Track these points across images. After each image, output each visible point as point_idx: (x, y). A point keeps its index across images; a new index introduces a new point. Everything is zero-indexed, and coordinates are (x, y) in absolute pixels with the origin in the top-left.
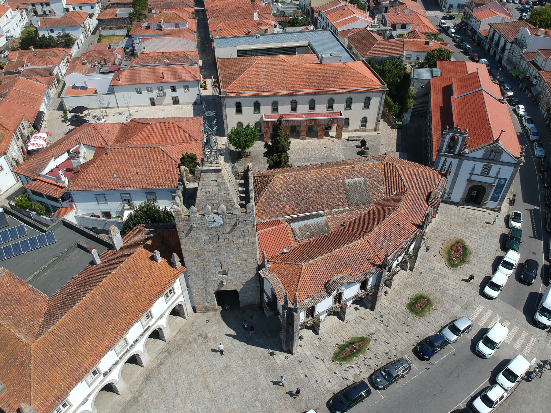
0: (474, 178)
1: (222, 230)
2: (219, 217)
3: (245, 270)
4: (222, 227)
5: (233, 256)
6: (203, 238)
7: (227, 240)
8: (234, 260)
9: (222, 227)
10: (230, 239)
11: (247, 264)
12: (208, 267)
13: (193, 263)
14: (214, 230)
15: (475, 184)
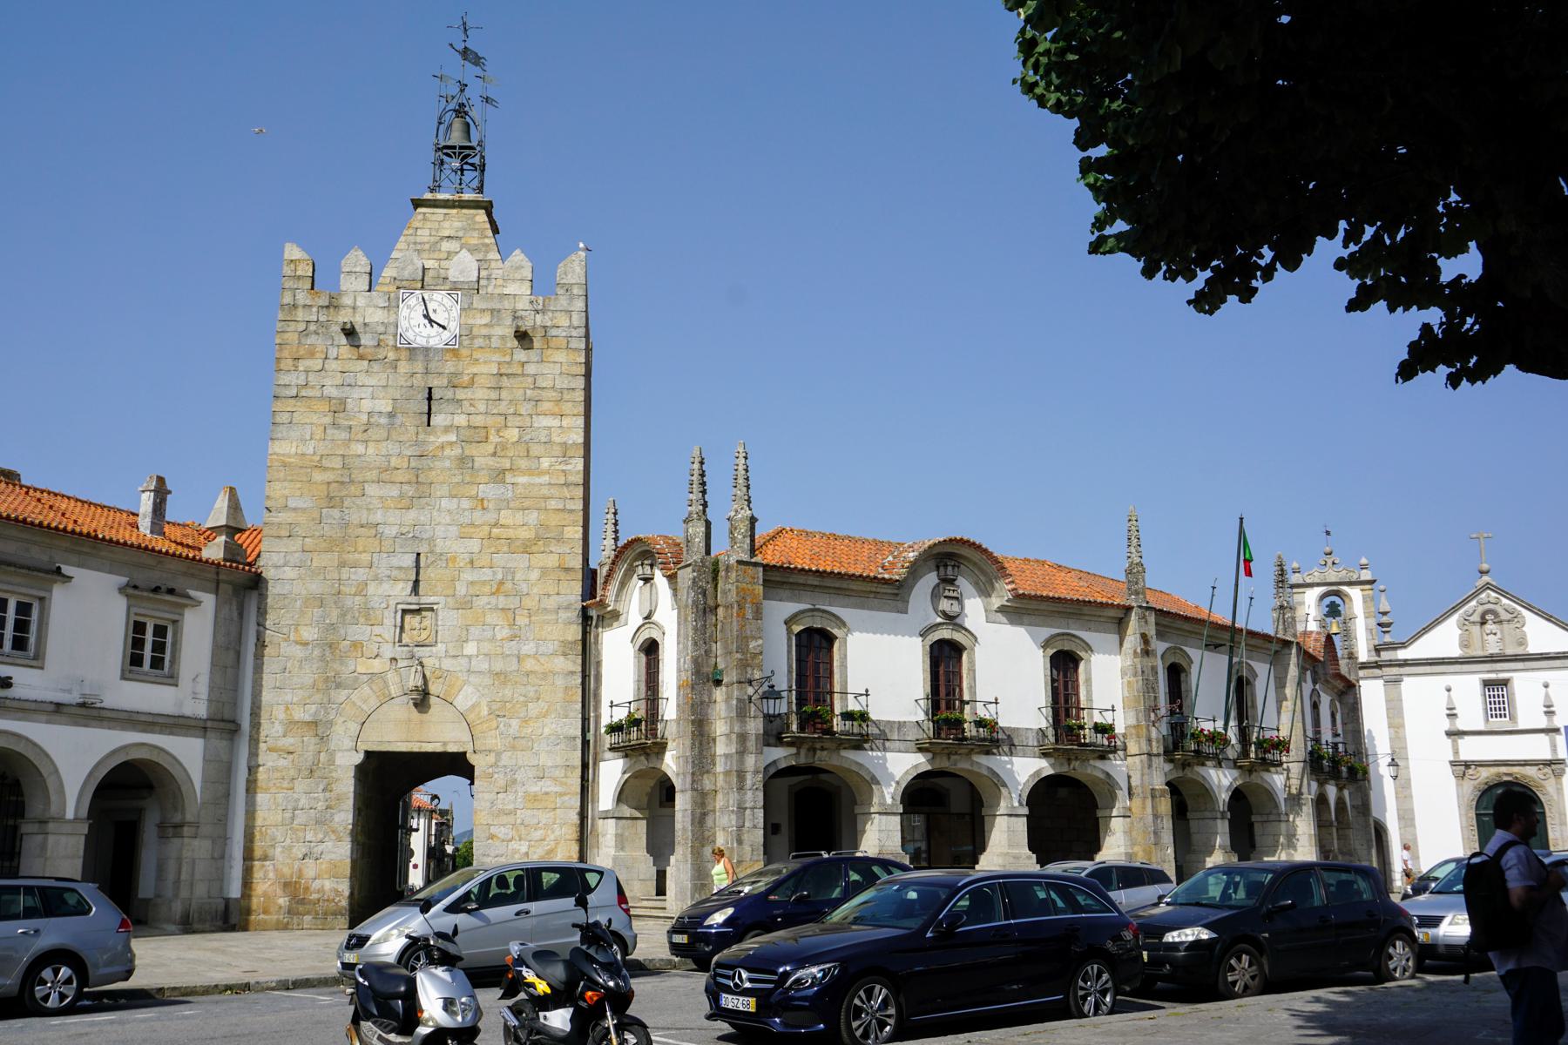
0: (1472, 749)
1: (449, 367)
2: (448, 302)
3: (522, 620)
4: (455, 353)
5: (478, 517)
6: (367, 405)
7: (461, 420)
8: (474, 545)
9: (455, 353)
10: (478, 420)
11: (535, 575)
12: (361, 574)
13: (296, 545)
14: (419, 367)
15: (1485, 774)
